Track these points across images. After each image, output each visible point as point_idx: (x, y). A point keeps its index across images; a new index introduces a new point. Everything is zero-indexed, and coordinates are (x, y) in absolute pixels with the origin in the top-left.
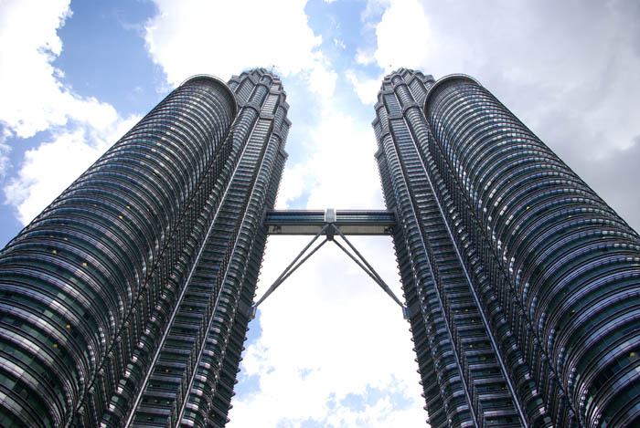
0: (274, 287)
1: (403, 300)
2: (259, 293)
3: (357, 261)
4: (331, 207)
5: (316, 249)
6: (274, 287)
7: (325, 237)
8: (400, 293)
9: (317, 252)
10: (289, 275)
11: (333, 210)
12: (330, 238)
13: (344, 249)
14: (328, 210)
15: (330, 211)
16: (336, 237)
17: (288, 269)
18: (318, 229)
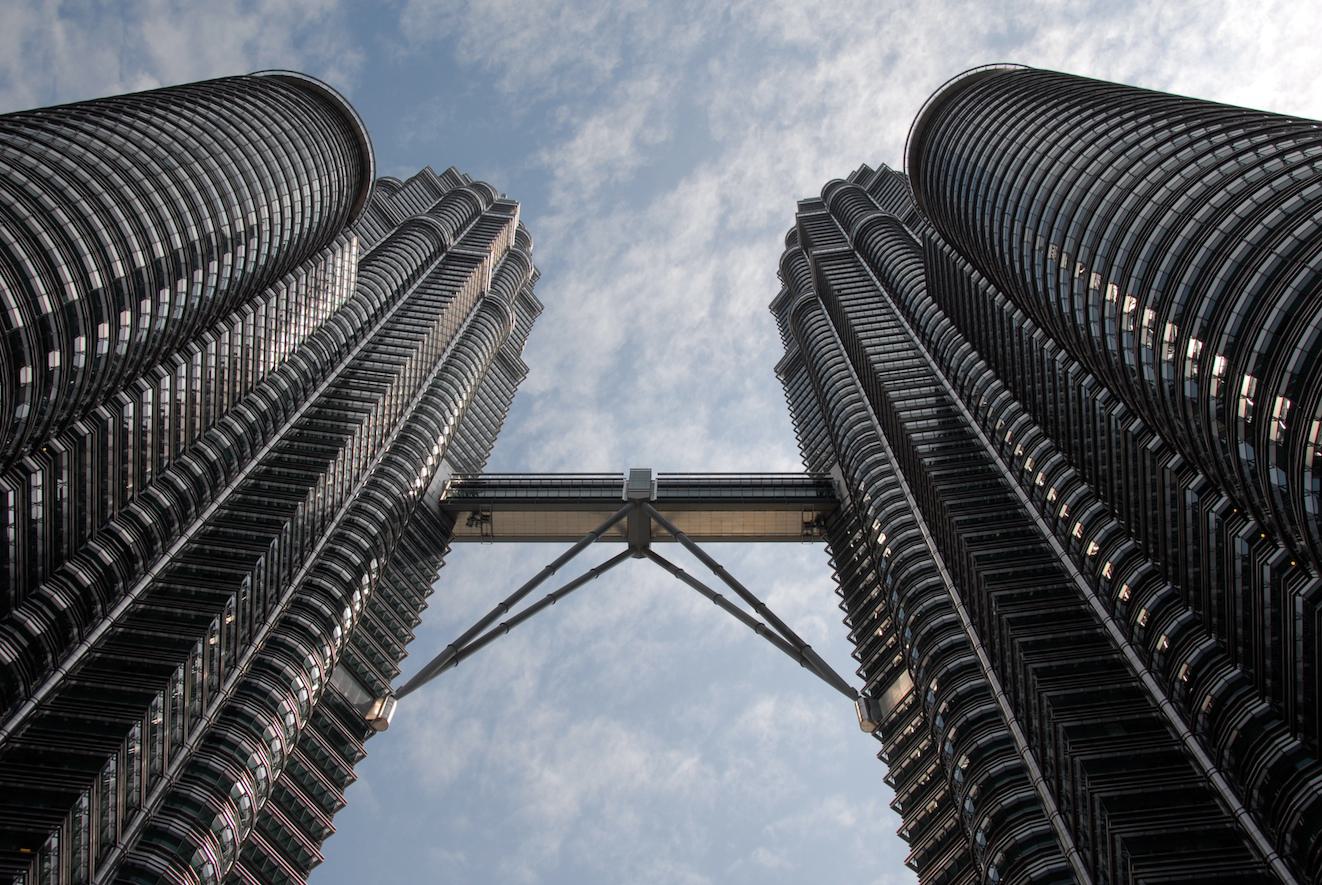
0: (457, 652)
1: (858, 684)
2: (408, 669)
3: (717, 598)
4: (643, 465)
5: (596, 572)
6: (457, 652)
7: (623, 547)
8: (848, 668)
9: (593, 583)
10: (506, 627)
11: (648, 473)
12: (639, 549)
13: (678, 573)
14: (635, 473)
15: (640, 475)
16: (655, 547)
17: (505, 606)
18: (591, 521)
